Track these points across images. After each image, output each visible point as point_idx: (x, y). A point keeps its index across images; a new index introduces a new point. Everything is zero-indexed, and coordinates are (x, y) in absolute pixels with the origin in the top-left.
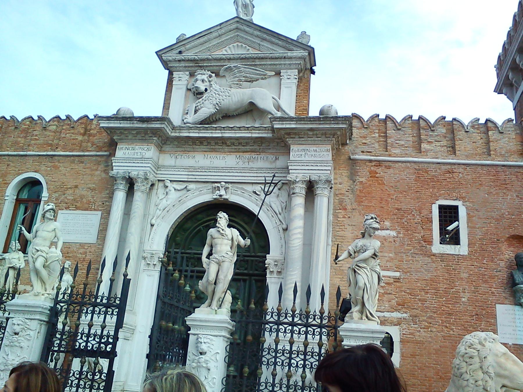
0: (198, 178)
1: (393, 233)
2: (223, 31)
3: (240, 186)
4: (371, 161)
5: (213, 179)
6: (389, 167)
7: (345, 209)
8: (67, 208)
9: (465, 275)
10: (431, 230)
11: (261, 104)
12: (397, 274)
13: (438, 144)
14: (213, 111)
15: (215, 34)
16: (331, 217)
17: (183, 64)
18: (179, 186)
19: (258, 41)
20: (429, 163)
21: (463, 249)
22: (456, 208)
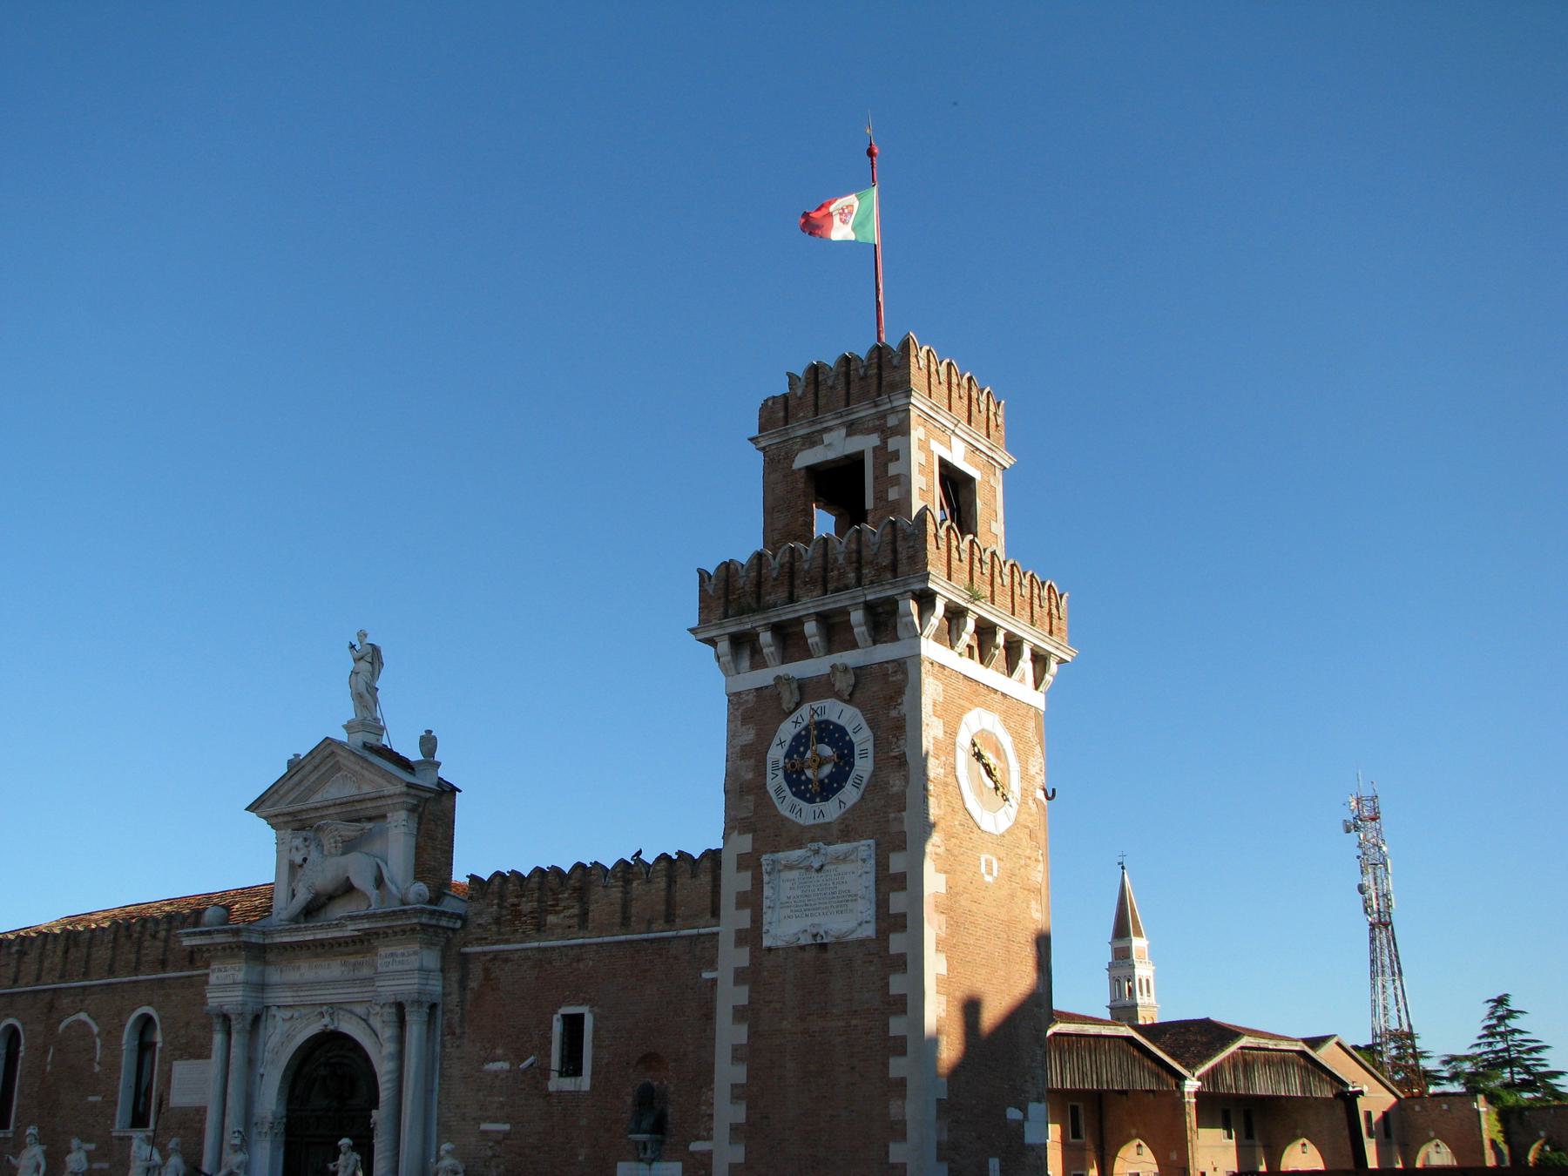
0: (307, 1000)
1: (505, 1065)
2: (317, 761)
3: (348, 1007)
4: (485, 954)
5: (318, 1000)
6: (506, 960)
7: (454, 1034)
8: (181, 1057)
9: (584, 1122)
10: (549, 1056)
11: (356, 882)
12: (507, 1127)
13: (567, 913)
14: (310, 896)
15: (309, 768)
16: (438, 1048)
17: (281, 819)
18: (287, 1014)
19: (358, 768)
20: (553, 948)
21: (584, 1082)
22: (582, 1016)
